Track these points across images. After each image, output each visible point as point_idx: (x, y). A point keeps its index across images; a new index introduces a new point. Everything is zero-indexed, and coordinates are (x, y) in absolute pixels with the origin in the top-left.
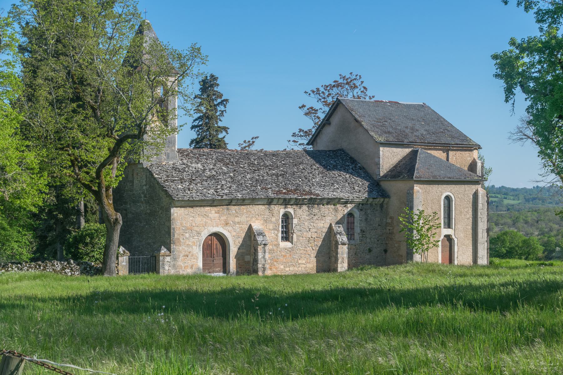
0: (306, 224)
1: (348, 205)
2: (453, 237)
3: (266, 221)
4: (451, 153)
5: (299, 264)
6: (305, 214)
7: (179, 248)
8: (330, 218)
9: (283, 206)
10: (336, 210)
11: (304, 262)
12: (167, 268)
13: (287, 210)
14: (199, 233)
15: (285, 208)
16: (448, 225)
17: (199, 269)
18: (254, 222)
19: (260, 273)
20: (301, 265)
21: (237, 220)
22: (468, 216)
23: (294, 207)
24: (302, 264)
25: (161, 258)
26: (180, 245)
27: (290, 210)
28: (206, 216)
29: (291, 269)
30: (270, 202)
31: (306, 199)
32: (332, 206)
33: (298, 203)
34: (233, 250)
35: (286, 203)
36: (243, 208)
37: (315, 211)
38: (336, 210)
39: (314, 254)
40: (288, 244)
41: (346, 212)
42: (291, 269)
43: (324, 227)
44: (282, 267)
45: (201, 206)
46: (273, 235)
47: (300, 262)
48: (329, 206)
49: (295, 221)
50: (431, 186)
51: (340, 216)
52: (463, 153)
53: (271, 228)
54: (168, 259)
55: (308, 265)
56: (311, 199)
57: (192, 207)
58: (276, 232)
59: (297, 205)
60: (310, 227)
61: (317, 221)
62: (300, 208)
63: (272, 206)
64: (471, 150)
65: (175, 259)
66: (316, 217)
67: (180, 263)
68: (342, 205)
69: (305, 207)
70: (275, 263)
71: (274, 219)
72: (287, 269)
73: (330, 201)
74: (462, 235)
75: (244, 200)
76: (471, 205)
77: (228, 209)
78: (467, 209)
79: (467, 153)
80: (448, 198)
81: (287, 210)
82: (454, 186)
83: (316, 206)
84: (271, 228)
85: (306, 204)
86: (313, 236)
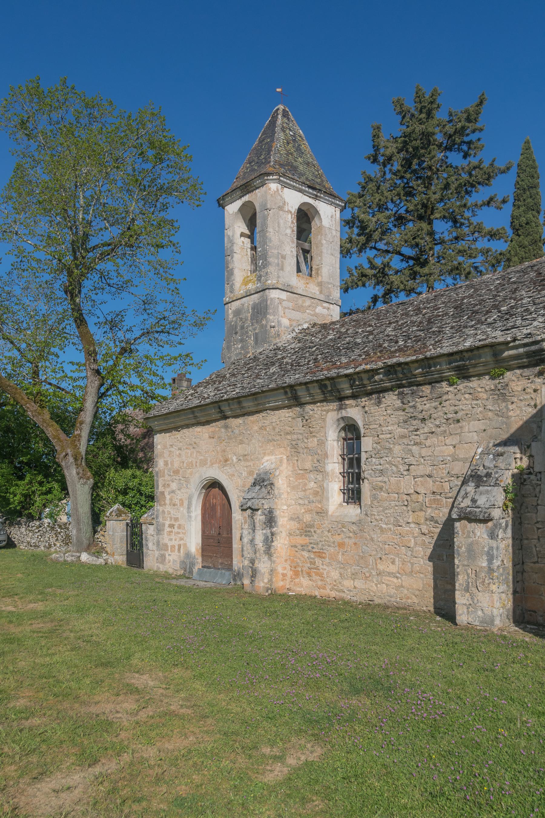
0: (397, 450)
3: (295, 447)
5: (379, 574)
8: (480, 425)
9: (334, 405)
10: (502, 394)
11: (393, 568)
13: (344, 413)
14: (187, 481)
15: (340, 408)
17: (188, 555)
18: (272, 453)
20: (386, 579)
21: (240, 449)
23: (364, 401)
24: (390, 574)
25: (144, 527)
26: (165, 504)
27: (354, 412)
29: (359, 584)
31: (375, 372)
32: (486, 382)
33: (363, 387)
35: (331, 391)
36: (254, 422)
37: (425, 405)
38: (502, 394)
39: (423, 543)
40: (353, 511)
42: (359, 584)
43: (455, 459)
44: (335, 574)
45: (188, 426)
46: (312, 484)
47: (381, 567)
48: (474, 383)
53: (308, 465)
55: (406, 581)
56: (390, 370)
58: (320, 477)
59: (369, 394)
60: (412, 460)
61: (433, 440)
62: (379, 403)
63: (308, 408)
65: (159, 531)
66: (430, 426)
68: (527, 372)
69: (391, 399)
70: (318, 561)
71: (313, 443)
72: (348, 583)
73: (462, 366)
75: (238, 399)
77: (226, 427)
81: (344, 413)
83: (426, 389)
84: (308, 465)
85: (391, 389)
86: (421, 490)
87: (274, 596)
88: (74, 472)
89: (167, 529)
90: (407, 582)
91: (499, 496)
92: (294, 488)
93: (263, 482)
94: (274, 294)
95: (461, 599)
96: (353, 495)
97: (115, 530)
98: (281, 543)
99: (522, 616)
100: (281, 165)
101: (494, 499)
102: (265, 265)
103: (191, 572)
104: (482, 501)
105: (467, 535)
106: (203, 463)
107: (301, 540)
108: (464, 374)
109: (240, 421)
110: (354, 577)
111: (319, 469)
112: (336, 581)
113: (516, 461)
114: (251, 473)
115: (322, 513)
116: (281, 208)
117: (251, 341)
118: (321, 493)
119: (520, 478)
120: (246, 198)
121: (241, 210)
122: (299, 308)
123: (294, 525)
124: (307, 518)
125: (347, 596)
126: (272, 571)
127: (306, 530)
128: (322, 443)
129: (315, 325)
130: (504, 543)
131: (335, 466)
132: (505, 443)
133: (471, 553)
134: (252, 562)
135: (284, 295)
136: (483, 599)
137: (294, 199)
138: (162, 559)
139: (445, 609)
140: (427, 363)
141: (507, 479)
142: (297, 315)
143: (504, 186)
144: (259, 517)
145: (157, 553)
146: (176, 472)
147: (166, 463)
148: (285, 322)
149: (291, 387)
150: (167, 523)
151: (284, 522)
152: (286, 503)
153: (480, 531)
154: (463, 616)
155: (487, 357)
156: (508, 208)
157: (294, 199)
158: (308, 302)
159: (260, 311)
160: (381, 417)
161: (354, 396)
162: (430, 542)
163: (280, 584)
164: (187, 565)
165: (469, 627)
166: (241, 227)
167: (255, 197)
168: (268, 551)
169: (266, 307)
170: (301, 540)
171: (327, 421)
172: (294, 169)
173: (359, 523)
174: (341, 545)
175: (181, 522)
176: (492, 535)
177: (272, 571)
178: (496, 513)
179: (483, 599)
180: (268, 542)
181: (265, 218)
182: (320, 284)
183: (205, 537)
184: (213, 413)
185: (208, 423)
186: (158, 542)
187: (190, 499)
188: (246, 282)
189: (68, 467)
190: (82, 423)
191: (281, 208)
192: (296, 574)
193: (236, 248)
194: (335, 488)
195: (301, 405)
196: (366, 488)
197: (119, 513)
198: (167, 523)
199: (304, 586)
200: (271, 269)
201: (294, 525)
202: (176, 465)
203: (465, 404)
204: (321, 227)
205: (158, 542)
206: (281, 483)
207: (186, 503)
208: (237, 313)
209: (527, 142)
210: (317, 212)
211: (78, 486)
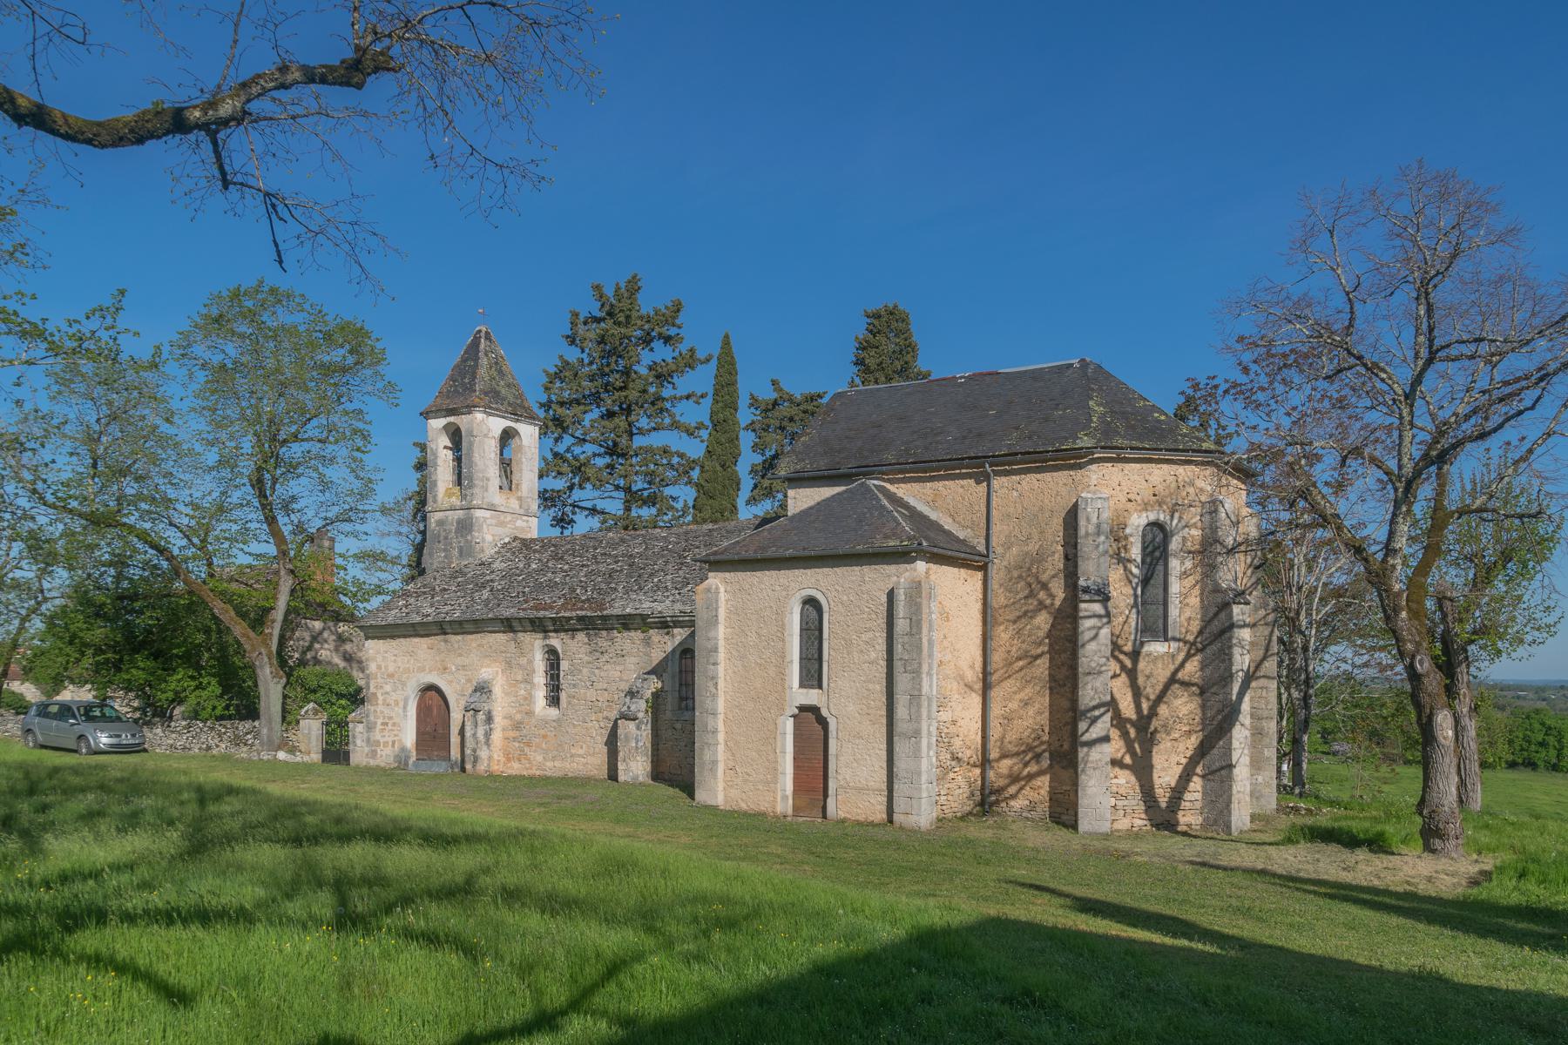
1: (676, 631)
2: (824, 712)
3: (509, 664)
4: (997, 482)
6: (583, 650)
7: (376, 710)
9: (540, 635)
10: (647, 642)
11: (581, 752)
12: (359, 742)
14: (404, 684)
16: (812, 675)
17: (403, 749)
19: (468, 767)
21: (459, 661)
22: (873, 655)
27: (555, 641)
28: (412, 654)
30: (509, 625)
34: (456, 716)
35: (538, 626)
36: (473, 640)
37: (602, 643)
38: (647, 642)
40: (553, 712)
41: (669, 648)
44: (540, 758)
45: (405, 636)
48: (633, 634)
49: (564, 665)
50: (758, 574)
51: (657, 655)
52: (1047, 476)
53: (519, 678)
54: (360, 728)
55: (590, 760)
56: (581, 619)
57: (393, 637)
64: (1080, 467)
65: (370, 728)
67: (377, 735)
69: (581, 636)
70: (526, 749)
71: (523, 661)
72: (549, 764)
73: (626, 623)
74: (851, 708)
75: (460, 623)
76: (882, 621)
78: (870, 635)
79: (1062, 476)
80: (811, 603)
82: (826, 570)
83: (604, 633)
84: (519, 678)
87: (492, 777)
88: (268, 671)
89: (379, 726)
90: (588, 759)
91: (642, 705)
92: (507, 694)
93: (483, 689)
94: (478, 513)
95: (621, 766)
96: (554, 700)
97: (311, 729)
98: (497, 736)
99: (657, 775)
100: (486, 394)
101: (640, 706)
102: (471, 486)
103: (406, 764)
104: (633, 708)
105: (627, 728)
106: (421, 669)
107: (512, 734)
108: (626, 627)
109: (459, 637)
110: (554, 758)
111: (528, 681)
112: (541, 762)
113: (654, 684)
114: (469, 681)
115: (530, 713)
116: (486, 436)
117: (456, 552)
118: (529, 699)
119: (656, 695)
120: (451, 419)
121: (446, 427)
122: (501, 524)
123: (507, 722)
124: (518, 717)
125: (549, 774)
126: (490, 758)
127: (517, 726)
128: (530, 662)
129: (515, 539)
130: (646, 732)
131: (540, 679)
132: (648, 673)
133: (627, 739)
134: (474, 751)
135: (488, 514)
136: (633, 765)
137: (497, 425)
138: (374, 754)
139: (613, 775)
140: (604, 618)
141: (648, 694)
142: (500, 531)
143: (701, 380)
144: (481, 716)
145: (366, 749)
146: (391, 676)
147: (379, 667)
148: (489, 538)
149: (508, 619)
150: (379, 721)
151: (499, 720)
152: (501, 705)
153: (632, 725)
154: (622, 778)
155: (638, 620)
156: (707, 403)
157: (497, 425)
158: (509, 517)
159: (465, 526)
160: (573, 648)
161: (556, 631)
162: (606, 733)
163: (495, 768)
164: (402, 760)
165: (626, 783)
166: (445, 441)
167: (462, 421)
168: (488, 743)
169: (471, 525)
170: (512, 734)
171: (535, 648)
172: (497, 393)
173: (558, 721)
174: (545, 737)
175: (396, 720)
176: (638, 728)
177: (490, 758)
178: (641, 715)
179: (633, 765)
180: (488, 735)
181: (471, 444)
182: (520, 499)
183: (420, 734)
184: (435, 629)
185: (427, 636)
186: (368, 740)
187: (406, 701)
188: (449, 494)
189: (262, 667)
190: (273, 621)
191: (486, 436)
192: (509, 760)
193: (440, 462)
194: (540, 695)
195: (514, 632)
196: (563, 696)
197: (316, 712)
198: (379, 721)
199: (515, 768)
200: (476, 490)
201: (507, 722)
202: (391, 669)
203: (627, 645)
204: (521, 447)
205: (368, 740)
206: (497, 690)
207: (401, 704)
208: (441, 523)
209: (727, 336)
210: (517, 433)
211: (272, 685)
